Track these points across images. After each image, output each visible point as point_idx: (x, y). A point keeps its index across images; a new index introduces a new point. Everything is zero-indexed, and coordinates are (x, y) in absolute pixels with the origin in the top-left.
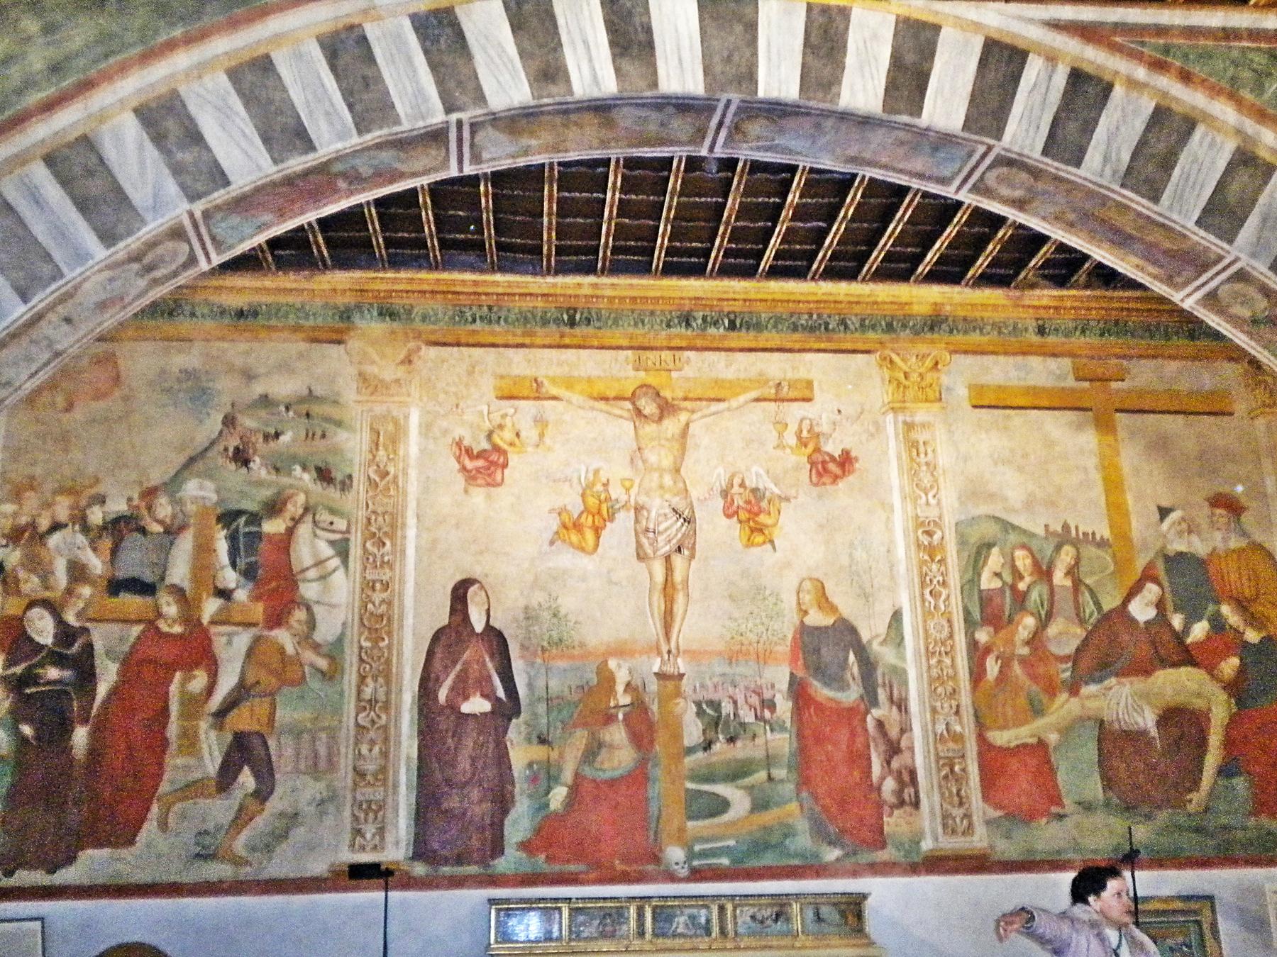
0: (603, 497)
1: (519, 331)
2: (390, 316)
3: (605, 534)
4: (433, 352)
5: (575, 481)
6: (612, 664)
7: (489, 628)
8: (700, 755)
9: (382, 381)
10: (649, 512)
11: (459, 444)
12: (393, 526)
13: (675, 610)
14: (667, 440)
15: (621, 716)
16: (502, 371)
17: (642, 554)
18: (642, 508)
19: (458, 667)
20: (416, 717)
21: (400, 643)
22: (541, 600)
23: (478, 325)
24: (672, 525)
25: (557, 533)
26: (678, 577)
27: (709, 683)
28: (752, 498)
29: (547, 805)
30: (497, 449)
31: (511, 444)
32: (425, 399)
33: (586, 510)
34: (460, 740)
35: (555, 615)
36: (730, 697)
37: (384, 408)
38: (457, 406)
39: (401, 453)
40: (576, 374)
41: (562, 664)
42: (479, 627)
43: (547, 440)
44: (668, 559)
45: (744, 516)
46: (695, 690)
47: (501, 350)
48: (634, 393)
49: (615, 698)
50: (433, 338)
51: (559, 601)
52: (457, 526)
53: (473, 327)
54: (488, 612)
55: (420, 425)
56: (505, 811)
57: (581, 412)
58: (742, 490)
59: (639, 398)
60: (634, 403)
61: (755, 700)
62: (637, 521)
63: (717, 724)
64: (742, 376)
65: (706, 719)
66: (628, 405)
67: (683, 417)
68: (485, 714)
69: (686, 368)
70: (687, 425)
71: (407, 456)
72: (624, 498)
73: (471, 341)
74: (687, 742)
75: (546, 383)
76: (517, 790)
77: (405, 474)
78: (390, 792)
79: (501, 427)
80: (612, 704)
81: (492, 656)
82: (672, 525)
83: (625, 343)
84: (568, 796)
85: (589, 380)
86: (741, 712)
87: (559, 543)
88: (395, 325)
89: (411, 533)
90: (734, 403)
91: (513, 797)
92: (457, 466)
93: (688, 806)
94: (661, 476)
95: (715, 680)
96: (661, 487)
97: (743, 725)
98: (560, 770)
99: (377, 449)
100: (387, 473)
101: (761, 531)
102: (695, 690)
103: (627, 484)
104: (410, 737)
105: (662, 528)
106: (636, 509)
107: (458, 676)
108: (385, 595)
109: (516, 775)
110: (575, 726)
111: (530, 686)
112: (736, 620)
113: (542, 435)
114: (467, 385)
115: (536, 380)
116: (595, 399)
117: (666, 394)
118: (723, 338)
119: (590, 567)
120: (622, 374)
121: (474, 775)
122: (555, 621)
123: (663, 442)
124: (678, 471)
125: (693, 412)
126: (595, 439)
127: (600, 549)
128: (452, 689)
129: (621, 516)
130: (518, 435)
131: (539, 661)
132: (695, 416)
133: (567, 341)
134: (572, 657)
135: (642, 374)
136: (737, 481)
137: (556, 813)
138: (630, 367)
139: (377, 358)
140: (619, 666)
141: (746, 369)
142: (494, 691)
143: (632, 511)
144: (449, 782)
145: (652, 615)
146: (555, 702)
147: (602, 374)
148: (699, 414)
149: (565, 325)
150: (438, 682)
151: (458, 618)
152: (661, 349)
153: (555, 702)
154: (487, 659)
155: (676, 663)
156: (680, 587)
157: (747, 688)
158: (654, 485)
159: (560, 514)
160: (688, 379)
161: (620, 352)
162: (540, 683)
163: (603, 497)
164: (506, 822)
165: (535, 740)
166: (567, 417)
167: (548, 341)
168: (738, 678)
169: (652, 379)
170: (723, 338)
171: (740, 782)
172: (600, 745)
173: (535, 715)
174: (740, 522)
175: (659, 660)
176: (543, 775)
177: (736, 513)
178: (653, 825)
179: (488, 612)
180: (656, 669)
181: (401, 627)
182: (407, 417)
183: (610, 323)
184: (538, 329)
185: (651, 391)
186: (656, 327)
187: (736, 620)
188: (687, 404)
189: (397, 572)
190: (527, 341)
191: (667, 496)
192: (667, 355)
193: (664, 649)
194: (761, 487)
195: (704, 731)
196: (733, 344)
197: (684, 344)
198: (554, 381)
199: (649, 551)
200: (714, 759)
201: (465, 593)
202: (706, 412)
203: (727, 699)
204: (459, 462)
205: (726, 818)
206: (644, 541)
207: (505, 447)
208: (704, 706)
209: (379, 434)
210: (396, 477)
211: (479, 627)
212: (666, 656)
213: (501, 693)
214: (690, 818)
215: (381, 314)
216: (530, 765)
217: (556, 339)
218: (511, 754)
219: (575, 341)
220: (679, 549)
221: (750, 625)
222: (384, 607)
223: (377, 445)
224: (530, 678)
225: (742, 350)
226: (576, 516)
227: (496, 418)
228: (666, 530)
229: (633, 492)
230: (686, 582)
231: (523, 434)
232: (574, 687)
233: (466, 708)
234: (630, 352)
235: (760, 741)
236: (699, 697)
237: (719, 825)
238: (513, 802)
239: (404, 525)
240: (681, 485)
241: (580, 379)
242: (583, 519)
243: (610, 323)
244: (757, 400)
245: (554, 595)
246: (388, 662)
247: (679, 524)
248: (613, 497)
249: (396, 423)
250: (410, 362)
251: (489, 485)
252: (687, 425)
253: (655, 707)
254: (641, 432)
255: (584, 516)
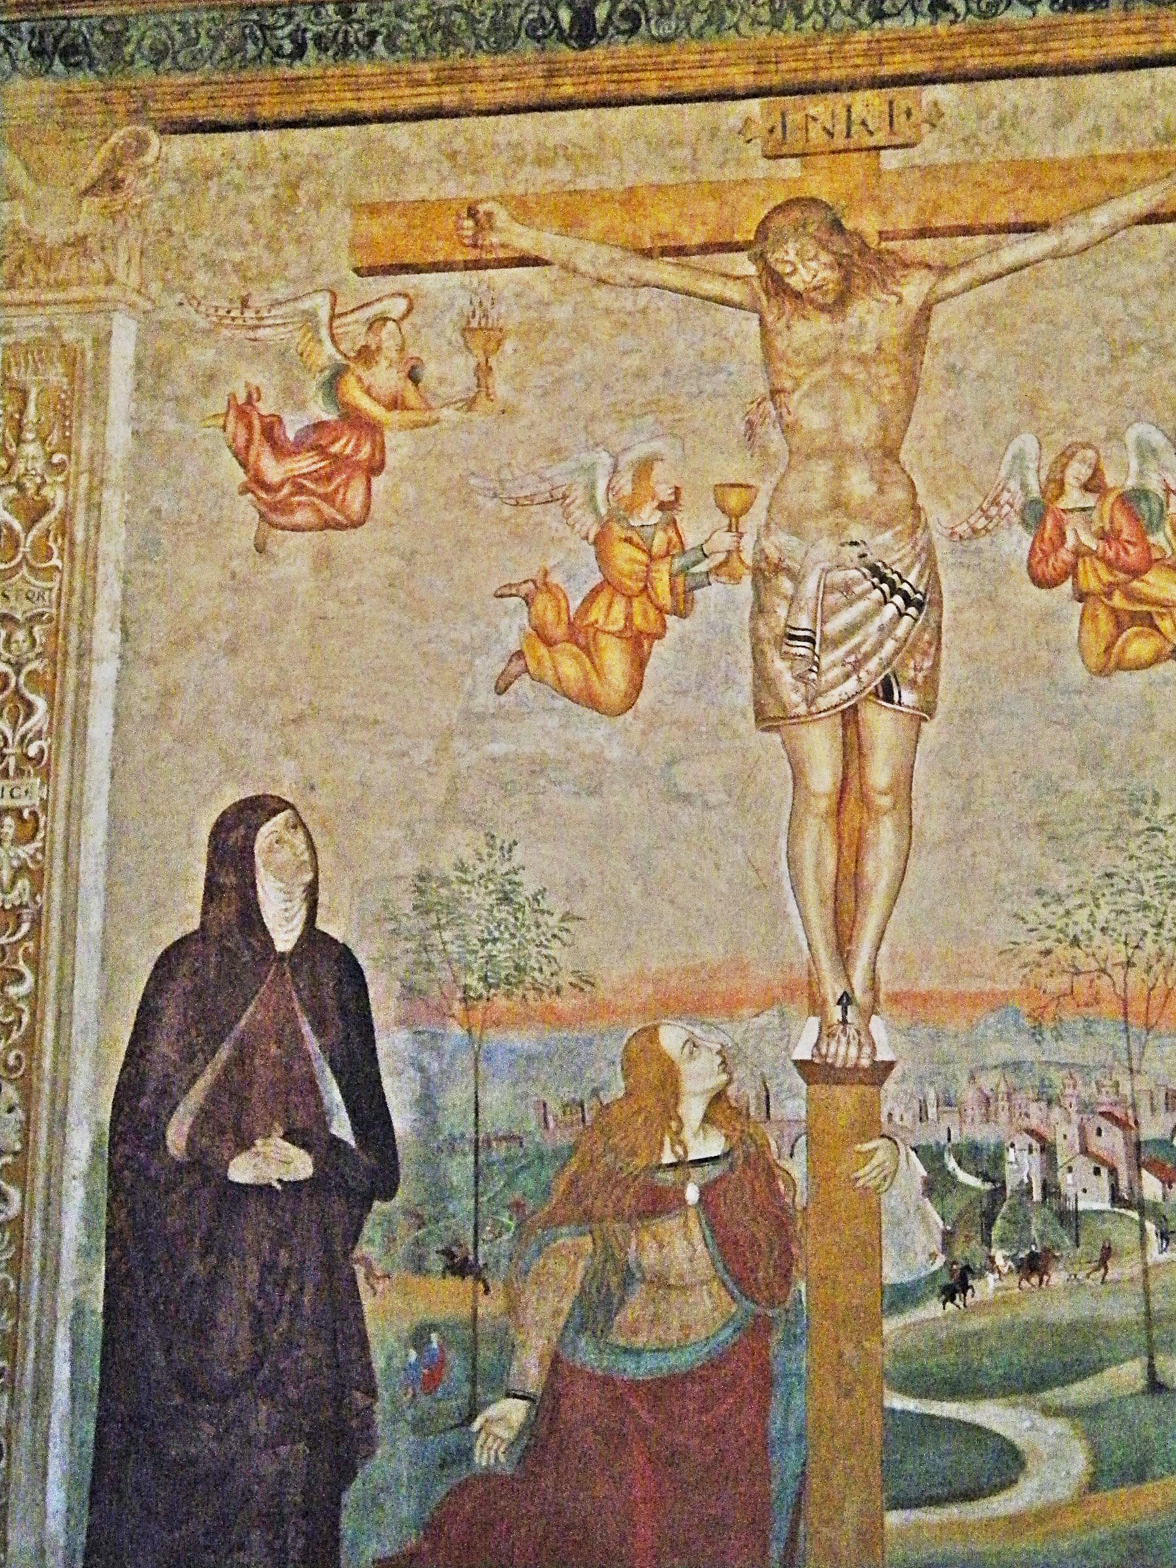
0: (659, 542)
1: (426, 71)
2: (65, 55)
3: (660, 652)
4: (181, 148)
5: (578, 494)
6: (671, 1038)
7: (312, 936)
8: (933, 1309)
9: (36, 246)
10: (796, 578)
11: (243, 411)
12: (54, 657)
13: (869, 867)
14: (862, 360)
15: (692, 1194)
16: (376, 192)
17: (773, 711)
18: (778, 568)
19: (224, 1053)
20: (103, 1197)
21: (65, 988)
22: (467, 854)
23: (310, 65)
24: (868, 617)
25: (519, 654)
26: (880, 774)
27: (969, 1095)
28: (1122, 520)
29: (465, 1454)
30: (354, 420)
31: (395, 404)
32: (155, 288)
33: (609, 585)
34: (223, 1259)
35: (506, 899)
36: (1031, 1132)
37: (39, 319)
38: (245, 304)
39: (85, 445)
40: (589, 183)
41: (523, 1039)
42: (285, 939)
43: (501, 389)
44: (850, 716)
45: (1093, 577)
46: (923, 1116)
47: (375, 128)
48: (763, 229)
49: (677, 1139)
50: (182, 111)
51: (518, 855)
52: (232, 649)
53: (299, 69)
54: (312, 890)
55: (139, 365)
56: (345, 1472)
57: (602, 296)
58: (1090, 500)
59: (781, 241)
60: (760, 258)
61: (1112, 1142)
62: (760, 610)
63: (989, 1219)
64: (1106, 149)
65: (957, 1203)
66: (743, 265)
67: (914, 289)
68: (296, 1185)
69: (929, 139)
70: (925, 312)
71: (99, 454)
72: (726, 540)
73: (292, 110)
74: (892, 1274)
75: (502, 217)
76: (382, 1408)
77: (95, 507)
78: (26, 1407)
79: (366, 355)
80: (668, 1158)
81: (320, 1027)
82: (868, 617)
83: (739, 77)
84: (528, 1427)
85: (630, 199)
86: (1067, 1182)
87: (523, 685)
88: (82, 80)
89: (104, 673)
90: (1076, 235)
91: (369, 1425)
92: (241, 476)
93: (891, 1471)
94: (839, 472)
95: (989, 1081)
96: (837, 503)
97: (1071, 1219)
98: (508, 1349)
99: (19, 441)
100: (45, 508)
101: (1148, 621)
102: (923, 1116)
103: (734, 500)
104: (85, 1252)
105: (835, 626)
106: (757, 571)
107: (219, 1085)
108: (25, 851)
109: (379, 1363)
110: (552, 1222)
111: (427, 1104)
112: (1059, 899)
113: (483, 371)
114: (273, 244)
115: (472, 213)
116: (647, 254)
117: (867, 223)
118: (1049, 30)
119: (614, 753)
120: (731, 173)
121: (258, 1360)
122: (502, 913)
123: (847, 368)
124: (891, 453)
125: (945, 271)
126: (641, 375)
127: (643, 701)
128: (204, 1116)
129: (710, 597)
130: (413, 376)
131: (456, 1030)
132: (951, 284)
133: (567, 89)
134: (558, 1020)
135: (791, 168)
136: (1077, 472)
137: (487, 1476)
138: (755, 150)
139: (26, 184)
140: (692, 1044)
141: (1119, 127)
142: (322, 1118)
143: (747, 580)
144: (185, 1382)
145: (796, 887)
146: (500, 1151)
147: (669, 179)
148: (964, 276)
149: (563, 38)
150: (168, 1099)
151: (227, 912)
152: (853, 86)
153: (500, 1151)
154: (306, 1029)
155: (866, 1038)
156: (885, 801)
157: (1086, 1107)
158: (817, 499)
159: (528, 601)
160: (930, 172)
161: (728, 105)
162: (456, 1097)
163: (659, 542)
164: (348, 1498)
165: (436, 1263)
166: (561, 313)
167: (509, 93)
168: (1057, 1077)
169: (819, 186)
170: (1049, 30)
171: (1054, 1396)
172: (628, 1277)
173: (439, 1192)
174: (1081, 597)
175: (814, 1021)
176: (456, 1366)
177: (1071, 571)
178: (781, 1527)
179: (312, 890)
180: (803, 1052)
181: (69, 937)
182: (102, 342)
183: (698, 20)
184: (482, 59)
185: (815, 217)
186: (837, 20)
187: (1059, 899)
188: (924, 248)
189: (63, 788)
190: (450, 97)
191: (856, 531)
192: (869, 104)
193: (832, 989)
194: (1154, 484)
195: (948, 1240)
196: (1077, 52)
197: (922, 66)
198: (522, 209)
199: (794, 698)
200: (975, 1323)
201: (250, 840)
202: (986, 267)
203: (1024, 1140)
204: (244, 465)
205: (1001, 1505)
206: (778, 665)
207: (376, 411)
208: (951, 1164)
209: (24, 394)
210: (67, 515)
211: (285, 939)
212: (836, 1013)
213: (342, 1128)
214: (898, 1504)
215: (37, 53)
216: (419, 1337)
217: (535, 87)
218: (368, 1303)
219: (593, 89)
220: (886, 692)
221: (1103, 914)
222: (23, 883)
223: (20, 427)
224: (427, 1081)
225: (1104, 67)
226: (575, 604)
227: (354, 331)
228: (851, 630)
229: (751, 523)
230: (904, 783)
231: (430, 372)
232: (554, 1107)
233: (241, 1171)
234: (754, 106)
235: (1123, 1269)
236: (933, 1135)
237: (988, 1524)
238: (371, 1442)
239: (84, 653)
240: (899, 495)
241: (601, 198)
242: (596, 614)
243: (698, 20)
244: (1152, 218)
245: (503, 837)
246: (30, 1041)
247: (890, 610)
248: (691, 540)
249: (72, 359)
250: (117, 186)
251: (327, 525)
252: (925, 312)
253: (797, 1168)
254: (780, 344)
255: (602, 600)
